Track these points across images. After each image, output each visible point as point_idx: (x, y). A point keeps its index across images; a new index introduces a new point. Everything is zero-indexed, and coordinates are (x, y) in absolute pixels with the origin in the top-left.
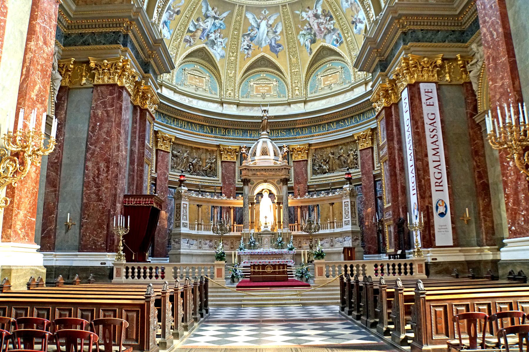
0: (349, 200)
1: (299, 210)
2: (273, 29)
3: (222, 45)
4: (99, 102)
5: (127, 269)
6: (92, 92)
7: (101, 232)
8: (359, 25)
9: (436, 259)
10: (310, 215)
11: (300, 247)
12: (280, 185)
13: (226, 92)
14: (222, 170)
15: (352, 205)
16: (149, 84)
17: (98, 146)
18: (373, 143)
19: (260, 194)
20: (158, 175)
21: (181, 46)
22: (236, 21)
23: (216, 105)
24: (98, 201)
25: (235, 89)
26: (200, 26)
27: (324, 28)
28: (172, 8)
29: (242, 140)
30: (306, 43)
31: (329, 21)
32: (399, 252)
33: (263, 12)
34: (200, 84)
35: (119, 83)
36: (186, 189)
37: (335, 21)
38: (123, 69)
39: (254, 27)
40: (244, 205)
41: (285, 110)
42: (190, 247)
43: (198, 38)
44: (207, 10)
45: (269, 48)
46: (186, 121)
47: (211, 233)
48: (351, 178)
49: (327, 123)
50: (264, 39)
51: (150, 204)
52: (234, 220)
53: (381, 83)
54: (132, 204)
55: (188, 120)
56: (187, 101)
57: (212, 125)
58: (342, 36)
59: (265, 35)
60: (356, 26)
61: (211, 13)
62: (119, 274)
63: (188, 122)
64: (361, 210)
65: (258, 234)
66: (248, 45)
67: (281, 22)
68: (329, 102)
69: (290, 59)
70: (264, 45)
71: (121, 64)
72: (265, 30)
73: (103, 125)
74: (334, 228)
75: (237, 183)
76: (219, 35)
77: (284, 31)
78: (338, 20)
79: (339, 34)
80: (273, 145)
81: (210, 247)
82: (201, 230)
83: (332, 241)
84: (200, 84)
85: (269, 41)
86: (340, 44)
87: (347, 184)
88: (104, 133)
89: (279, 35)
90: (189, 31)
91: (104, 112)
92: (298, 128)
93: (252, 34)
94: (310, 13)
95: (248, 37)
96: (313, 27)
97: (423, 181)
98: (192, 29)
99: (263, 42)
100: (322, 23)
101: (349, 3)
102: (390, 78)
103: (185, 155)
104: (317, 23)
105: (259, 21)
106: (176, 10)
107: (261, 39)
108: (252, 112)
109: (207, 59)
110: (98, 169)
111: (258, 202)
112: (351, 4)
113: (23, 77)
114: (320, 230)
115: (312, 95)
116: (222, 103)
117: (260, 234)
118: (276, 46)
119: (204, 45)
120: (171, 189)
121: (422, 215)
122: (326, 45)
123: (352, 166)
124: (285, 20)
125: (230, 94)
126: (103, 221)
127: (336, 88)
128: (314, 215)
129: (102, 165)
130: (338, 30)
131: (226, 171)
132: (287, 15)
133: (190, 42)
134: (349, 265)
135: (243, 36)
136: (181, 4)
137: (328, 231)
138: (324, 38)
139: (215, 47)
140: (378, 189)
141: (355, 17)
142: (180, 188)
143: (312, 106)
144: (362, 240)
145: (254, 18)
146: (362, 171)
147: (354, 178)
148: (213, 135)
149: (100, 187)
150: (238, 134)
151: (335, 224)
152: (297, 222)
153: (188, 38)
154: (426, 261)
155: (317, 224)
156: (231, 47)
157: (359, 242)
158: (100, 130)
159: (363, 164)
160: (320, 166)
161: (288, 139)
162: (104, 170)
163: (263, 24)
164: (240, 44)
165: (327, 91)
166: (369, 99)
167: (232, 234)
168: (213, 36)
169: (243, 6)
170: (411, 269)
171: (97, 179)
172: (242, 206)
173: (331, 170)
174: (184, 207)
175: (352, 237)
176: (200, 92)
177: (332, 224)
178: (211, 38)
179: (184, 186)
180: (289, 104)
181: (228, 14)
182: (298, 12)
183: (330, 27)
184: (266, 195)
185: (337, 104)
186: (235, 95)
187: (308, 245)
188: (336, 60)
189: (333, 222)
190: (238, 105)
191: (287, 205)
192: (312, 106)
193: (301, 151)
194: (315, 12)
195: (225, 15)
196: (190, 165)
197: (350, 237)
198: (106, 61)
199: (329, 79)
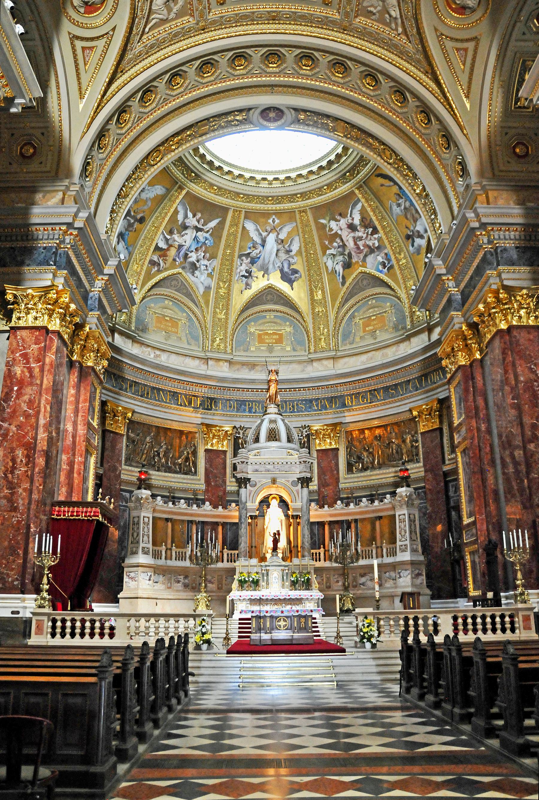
0: (405, 512)
1: (327, 527)
2: (286, 246)
3: (207, 270)
4: (18, 355)
5: (54, 621)
6: (8, 339)
7: (14, 561)
8: (418, 241)
12: (296, 488)
14: (206, 463)
15: (410, 520)
17: (15, 423)
18: (441, 422)
19: (265, 502)
20: (104, 472)
22: (229, 235)
23: (197, 362)
24: (11, 511)
26: (175, 241)
28: (132, 213)
31: (372, 234)
32: (490, 595)
33: (270, 221)
34: (174, 330)
39: (257, 243)
40: (240, 519)
41: (303, 371)
44: (186, 217)
48: (408, 477)
49: (370, 391)
50: (271, 262)
51: (94, 516)
52: (224, 543)
54: (64, 515)
56: (152, 356)
58: (393, 258)
59: (275, 254)
60: (413, 241)
61: (192, 221)
62: (40, 630)
64: (425, 528)
66: (247, 271)
68: (371, 359)
72: (273, 248)
73: (23, 391)
74: (382, 556)
75: (228, 483)
76: (203, 254)
77: (303, 249)
79: (386, 254)
80: (285, 424)
82: (171, 559)
85: (279, 264)
87: (402, 487)
88: (25, 402)
89: (296, 255)
90: (157, 248)
91: (25, 370)
93: (253, 254)
94: (343, 222)
95: (247, 259)
96: (347, 244)
97: (526, 481)
98: (162, 245)
100: (361, 238)
101: (403, 207)
102: (469, 321)
104: (354, 237)
105: (264, 234)
106: (139, 217)
107: (267, 261)
108: (252, 372)
109: (185, 291)
110: (14, 460)
111: (262, 515)
112: (405, 208)
114: (361, 560)
116: (207, 360)
118: (290, 272)
120: (124, 493)
121: (526, 535)
122: (368, 270)
124: (304, 232)
126: (18, 543)
128: (351, 536)
129: (20, 453)
131: (211, 466)
132: (306, 226)
133: (159, 264)
134: (411, 616)
135: (240, 256)
136: (146, 207)
139: (197, 273)
140: (451, 494)
141: (412, 228)
142: (139, 491)
143: (345, 363)
144: (428, 577)
145: (258, 230)
146: (424, 466)
147: (412, 476)
149: (14, 488)
150: (231, 407)
152: (324, 548)
153: (155, 258)
155: (356, 550)
157: (423, 579)
158: (18, 397)
162: (22, 461)
163: (271, 239)
166: (436, 354)
167: (220, 565)
169: (240, 211)
170: (512, 623)
171: (10, 476)
172: (237, 521)
175: (412, 571)
178: (190, 260)
179: (145, 489)
181: (218, 224)
182: (323, 221)
183: (374, 244)
184: (274, 503)
185: (385, 361)
186: (226, 347)
187: (340, 583)
189: (381, 547)
190: (230, 362)
191: (309, 520)
192: (345, 363)
194: (350, 221)
195: (213, 224)
199: (372, 323)
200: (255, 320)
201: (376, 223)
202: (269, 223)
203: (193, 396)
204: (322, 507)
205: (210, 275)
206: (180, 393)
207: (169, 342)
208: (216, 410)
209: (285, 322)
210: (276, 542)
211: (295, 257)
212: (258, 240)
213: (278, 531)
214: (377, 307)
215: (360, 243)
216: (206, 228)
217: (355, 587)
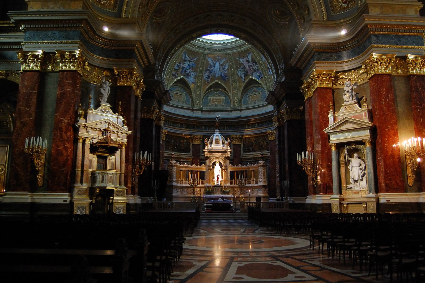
1: (235, 173)
2: (223, 67)
3: (193, 76)
5: (158, 204)
9: (294, 202)
10: (241, 177)
11: (236, 193)
13: (195, 103)
14: (193, 149)
16: (161, 113)
19: (214, 164)
21: (170, 79)
23: (189, 111)
25: (200, 101)
27: (252, 68)
29: (204, 131)
30: (242, 76)
31: (255, 65)
32: (281, 198)
34: (181, 99)
35: (151, 117)
36: (175, 161)
40: (206, 170)
41: (228, 114)
42: (177, 193)
43: (180, 73)
44: (185, 57)
47: (188, 185)
49: (252, 124)
50: (217, 73)
53: (277, 114)
56: (173, 110)
57: (187, 123)
59: (218, 70)
61: (188, 58)
63: (174, 122)
65: (213, 186)
66: (208, 76)
67: (228, 63)
69: (232, 84)
70: (217, 76)
71: (152, 109)
76: (192, 70)
77: (229, 68)
78: (260, 65)
79: (260, 73)
80: (222, 137)
81: (187, 193)
83: (252, 190)
84: (181, 99)
87: (261, 160)
89: (227, 70)
90: (175, 69)
93: (211, 69)
94: (245, 59)
98: (177, 68)
99: (217, 74)
100: (251, 66)
103: (173, 141)
104: (248, 65)
105: (215, 62)
111: (213, 168)
114: (246, 185)
115: (246, 106)
116: (192, 110)
117: (214, 186)
119: (183, 77)
122: (253, 78)
123: (265, 149)
124: (230, 62)
125: (197, 104)
127: (258, 103)
130: (260, 70)
133: (176, 75)
137: (250, 185)
148: (188, 129)
151: (255, 181)
152: (234, 180)
153: (174, 73)
154: (290, 203)
155: (245, 181)
156: (198, 77)
160: (248, 148)
161: (230, 131)
163: (217, 64)
164: (203, 75)
165: (252, 105)
167: (198, 186)
168: (188, 71)
173: (254, 150)
174: (174, 172)
176: (181, 104)
177: (253, 181)
178: (187, 72)
179: (174, 160)
180: (231, 111)
184: (217, 164)
186: (200, 105)
187: (239, 192)
188: (258, 86)
189: (254, 180)
190: (202, 111)
193: (237, 139)
194: (247, 59)
195: (195, 59)
196: (175, 147)
198: (145, 107)
201: (257, 62)
202: (217, 58)
203: (188, 124)
204: (234, 166)
205: (194, 78)
206: (183, 123)
207: (179, 104)
208: (196, 129)
209: (222, 95)
210: (218, 178)
211: (226, 71)
213: (219, 175)
214: (257, 91)
215: (251, 68)
216: (193, 61)
217: (244, 193)
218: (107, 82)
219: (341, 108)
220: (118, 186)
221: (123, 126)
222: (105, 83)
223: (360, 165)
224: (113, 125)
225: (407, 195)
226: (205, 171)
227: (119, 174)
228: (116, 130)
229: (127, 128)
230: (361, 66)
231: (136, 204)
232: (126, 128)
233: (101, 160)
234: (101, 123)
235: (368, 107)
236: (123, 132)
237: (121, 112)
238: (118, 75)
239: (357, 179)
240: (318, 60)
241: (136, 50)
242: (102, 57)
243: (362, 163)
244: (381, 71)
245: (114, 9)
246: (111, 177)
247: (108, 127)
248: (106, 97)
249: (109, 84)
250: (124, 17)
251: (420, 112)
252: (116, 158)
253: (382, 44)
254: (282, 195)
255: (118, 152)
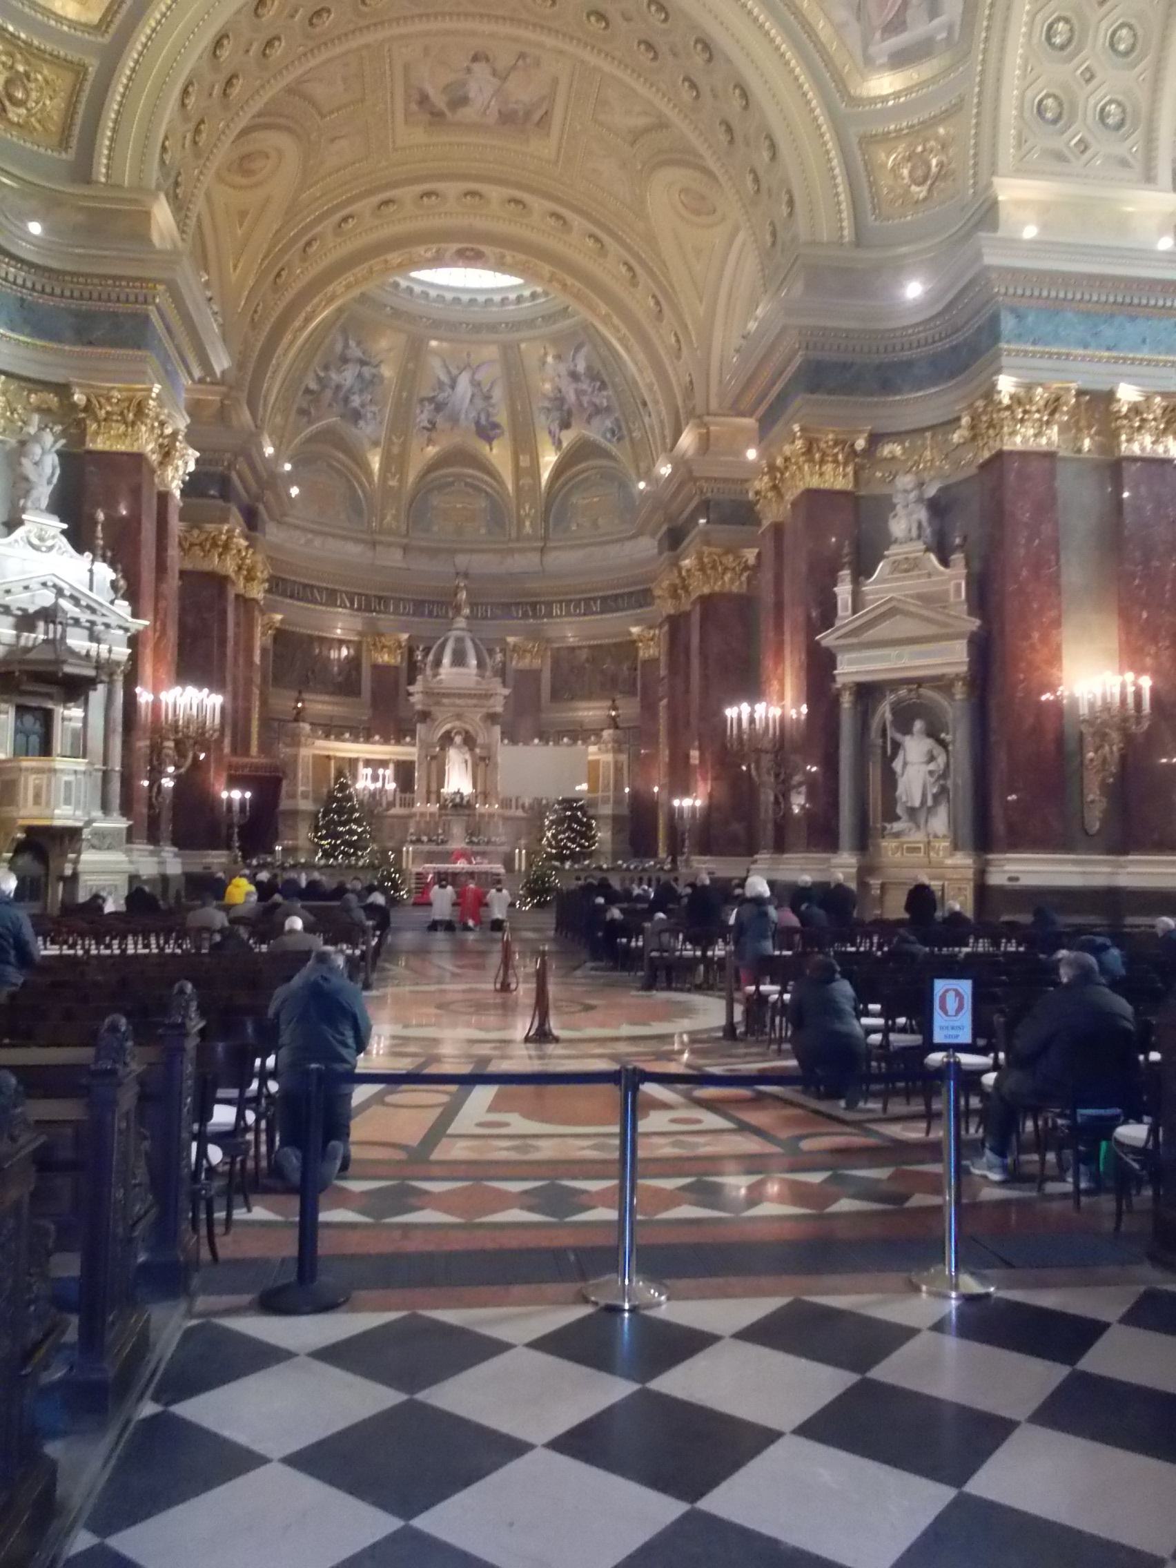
19: (447, 739)
26: (331, 379)
31: (600, 389)
37: (609, 392)
38: (226, 547)
44: (346, 346)
45: (473, 427)
46: (300, 583)
49: (585, 599)
55: (306, 581)
59: (467, 401)
66: (430, 422)
79: (617, 420)
86: (619, 439)
90: (308, 391)
92: (527, 603)
93: (441, 397)
98: (313, 386)
99: (463, 416)
100: (584, 392)
113: (157, 634)
133: (309, 413)
138: (588, 421)
139: (361, 423)
142: (295, 725)
153: (305, 405)
159: (644, 687)
175: (613, 828)
194: (572, 367)
197: (610, 827)
200: (440, 488)
201: (606, 379)
212: (445, 378)
215: (585, 400)
218: (48, 438)
219: (881, 565)
220: (98, 813)
221: (112, 602)
222: (36, 438)
223: (931, 758)
224: (72, 597)
225: (1075, 862)
226: (412, 763)
227: (100, 774)
228: (84, 617)
229: (129, 610)
230: (958, 419)
231: (164, 879)
232: (123, 607)
233: (29, 720)
234: (26, 588)
235: (967, 565)
236: (113, 620)
237: (104, 548)
238: (88, 408)
239: (917, 803)
240: (812, 392)
241: (154, 317)
242: (23, 334)
243: (938, 750)
244: (1021, 438)
245: (60, 145)
246: (68, 784)
247: (56, 604)
248: (43, 492)
249: (55, 442)
250: (105, 184)
251: (1139, 587)
252: (85, 720)
253: (1034, 343)
254: (675, 851)
255: (97, 696)
